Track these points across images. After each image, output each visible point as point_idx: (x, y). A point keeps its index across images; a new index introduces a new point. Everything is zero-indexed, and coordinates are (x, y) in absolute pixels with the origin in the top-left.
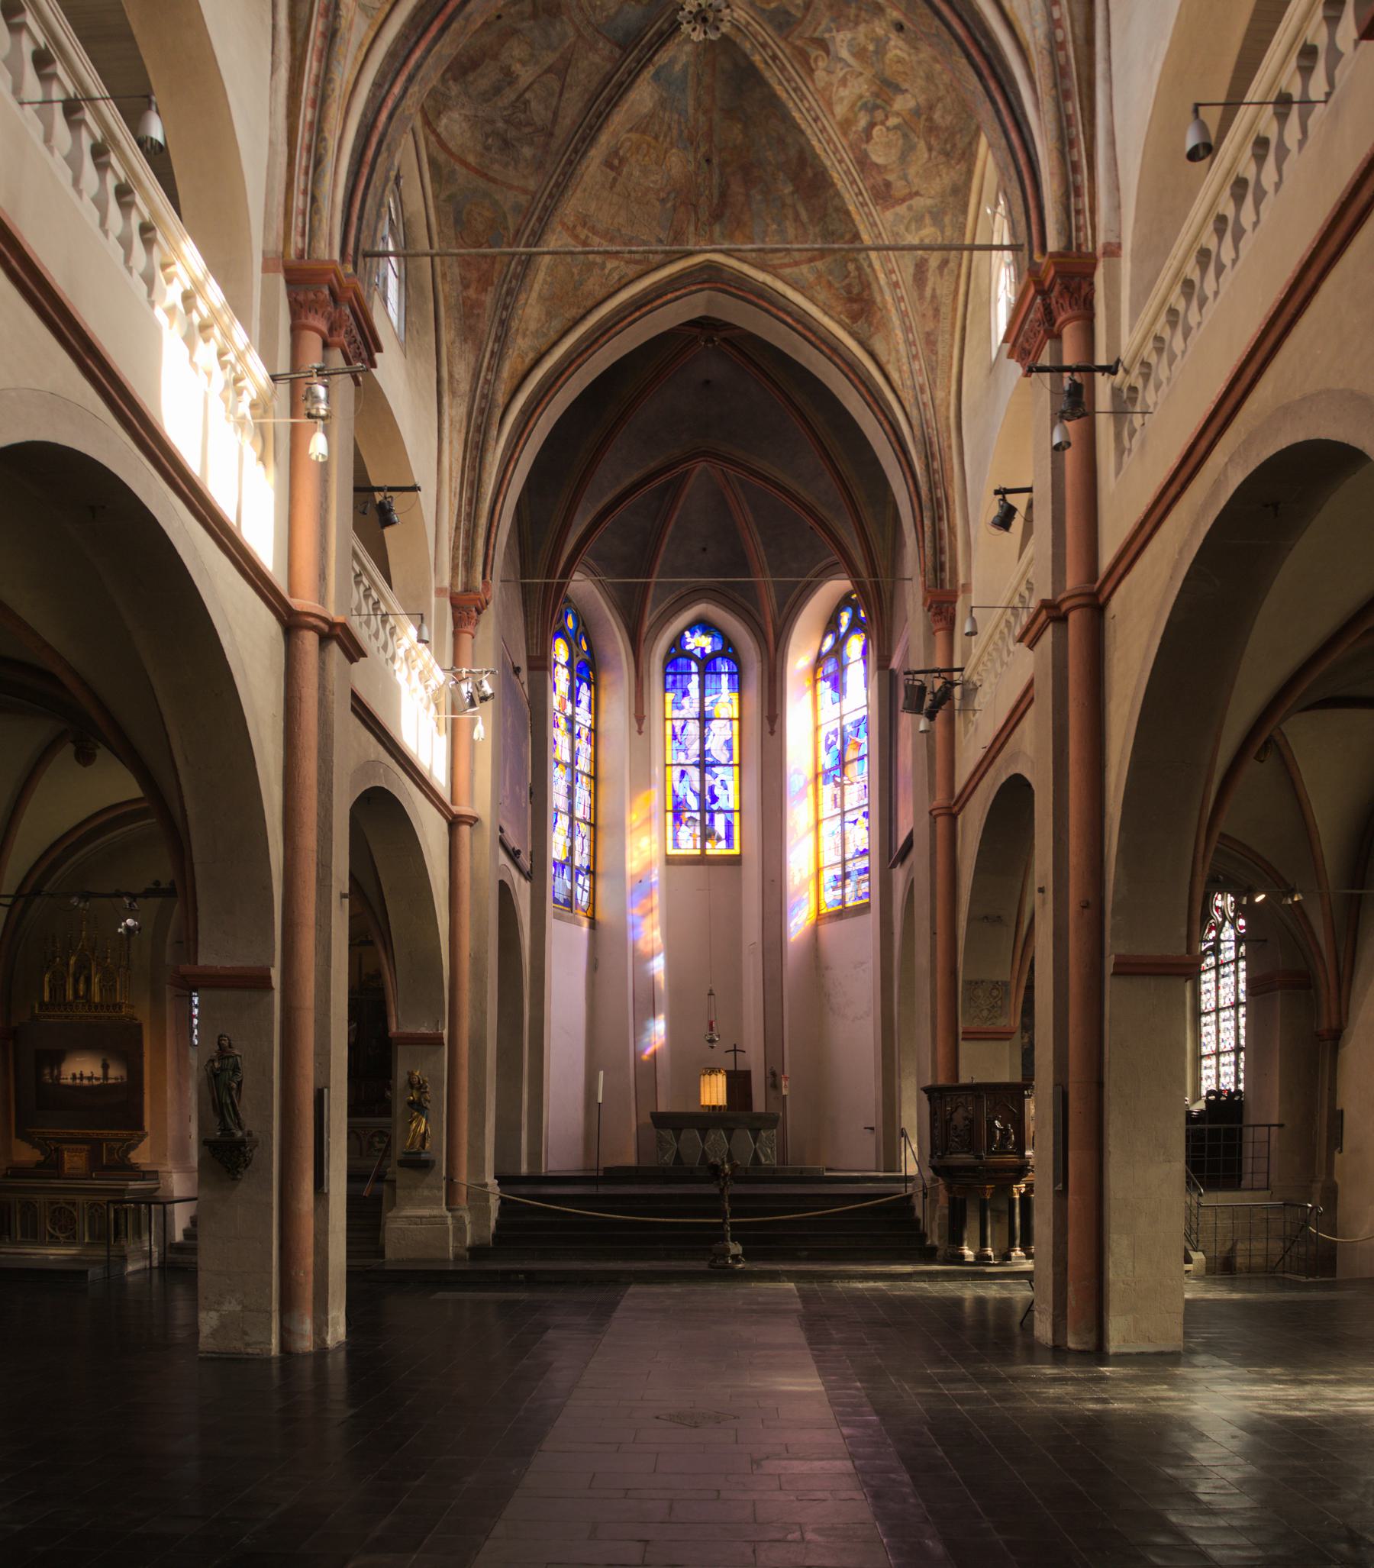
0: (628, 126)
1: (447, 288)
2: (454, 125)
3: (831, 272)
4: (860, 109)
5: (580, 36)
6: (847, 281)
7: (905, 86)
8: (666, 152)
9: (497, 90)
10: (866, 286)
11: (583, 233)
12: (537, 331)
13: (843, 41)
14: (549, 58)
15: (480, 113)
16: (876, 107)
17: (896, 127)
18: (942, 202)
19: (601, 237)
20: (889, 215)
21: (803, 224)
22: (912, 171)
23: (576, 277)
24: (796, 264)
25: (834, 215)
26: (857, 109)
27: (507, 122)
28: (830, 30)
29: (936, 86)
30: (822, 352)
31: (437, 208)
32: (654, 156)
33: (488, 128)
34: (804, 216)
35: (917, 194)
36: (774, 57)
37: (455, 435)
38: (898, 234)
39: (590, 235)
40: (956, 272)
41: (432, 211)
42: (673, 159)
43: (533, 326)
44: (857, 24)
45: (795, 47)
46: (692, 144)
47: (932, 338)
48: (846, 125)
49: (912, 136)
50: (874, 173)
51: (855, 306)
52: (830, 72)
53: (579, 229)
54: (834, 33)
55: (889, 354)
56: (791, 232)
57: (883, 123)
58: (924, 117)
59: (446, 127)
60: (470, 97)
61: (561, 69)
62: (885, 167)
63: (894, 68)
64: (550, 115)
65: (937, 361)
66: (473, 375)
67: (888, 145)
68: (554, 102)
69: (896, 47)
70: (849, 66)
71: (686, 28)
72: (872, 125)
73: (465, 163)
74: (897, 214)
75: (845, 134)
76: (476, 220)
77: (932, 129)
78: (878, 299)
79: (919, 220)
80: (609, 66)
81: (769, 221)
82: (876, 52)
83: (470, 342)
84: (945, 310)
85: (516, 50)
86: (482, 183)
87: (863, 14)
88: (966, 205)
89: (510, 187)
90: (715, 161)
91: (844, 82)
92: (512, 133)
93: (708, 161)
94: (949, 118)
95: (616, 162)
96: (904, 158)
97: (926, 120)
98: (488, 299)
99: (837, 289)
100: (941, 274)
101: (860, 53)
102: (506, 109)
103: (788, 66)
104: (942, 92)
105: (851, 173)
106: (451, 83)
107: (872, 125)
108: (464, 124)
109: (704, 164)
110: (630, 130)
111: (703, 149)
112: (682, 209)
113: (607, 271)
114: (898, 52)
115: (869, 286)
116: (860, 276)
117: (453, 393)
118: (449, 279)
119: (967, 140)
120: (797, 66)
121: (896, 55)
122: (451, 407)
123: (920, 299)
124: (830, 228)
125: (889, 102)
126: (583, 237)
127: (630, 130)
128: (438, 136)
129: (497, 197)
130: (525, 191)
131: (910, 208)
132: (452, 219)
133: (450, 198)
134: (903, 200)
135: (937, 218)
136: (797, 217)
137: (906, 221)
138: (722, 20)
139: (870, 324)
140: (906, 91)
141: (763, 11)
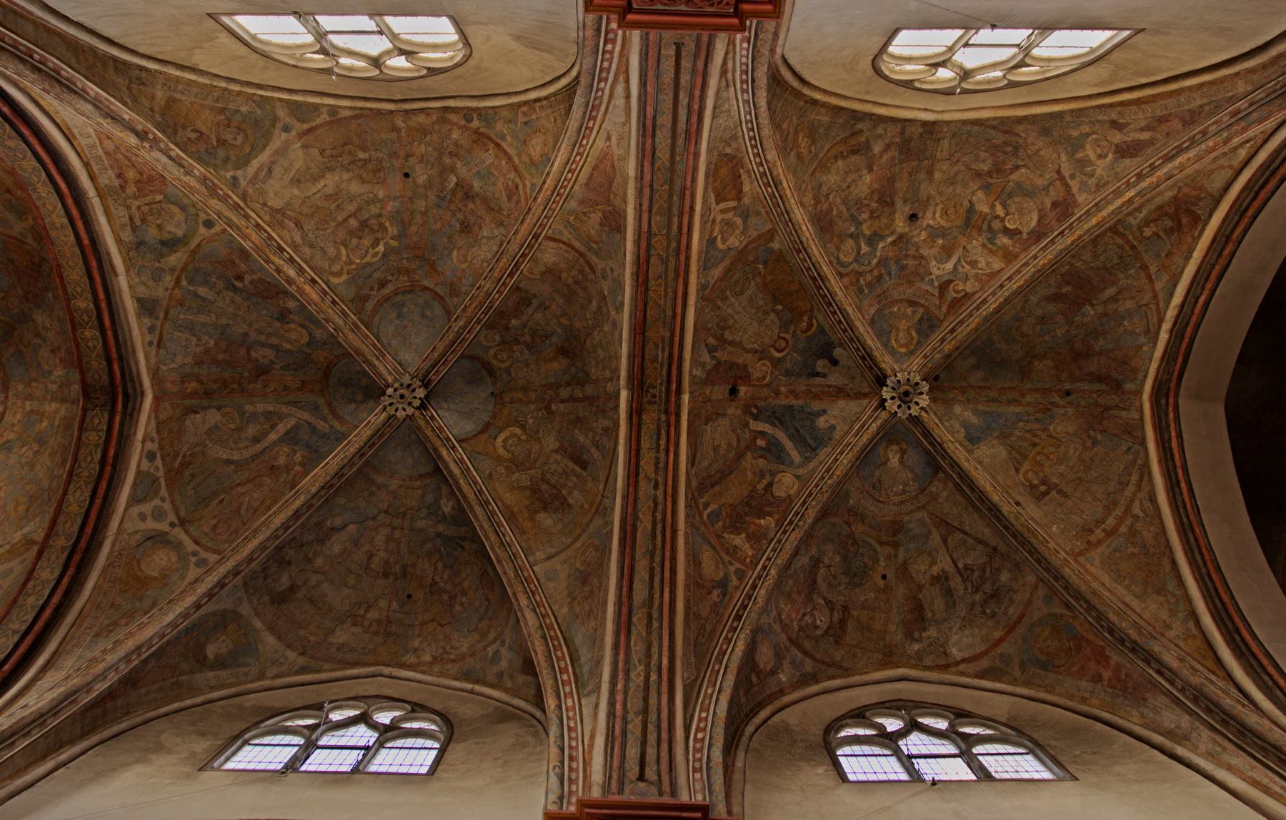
0: (1013, 472)
1: (1095, 701)
2: (961, 643)
3: (1158, 256)
4: (995, 244)
5: (924, 507)
6: (1162, 234)
7: (966, 203)
8: (1051, 436)
9: (949, 593)
10: (1161, 212)
11: (1099, 533)
12: (1170, 610)
13: (939, 269)
14: (936, 538)
15: (962, 614)
16: (990, 228)
17: (1004, 206)
18: (1061, 144)
19: (1110, 514)
20: (1081, 198)
21: (1119, 292)
22: (1040, 182)
23: (1136, 550)
24: (1155, 296)
25: (1102, 258)
26: (994, 248)
27: (977, 591)
28: (932, 281)
29: (957, 173)
30: (1233, 254)
31: (1026, 684)
32: (1052, 449)
33: (978, 609)
34: (1111, 291)
35: (1059, 172)
36: (952, 331)
37: (1225, 757)
38: (1097, 185)
39: (1103, 526)
40: (1119, 108)
41: (1019, 690)
42: (1058, 429)
43: (1164, 614)
44: (922, 257)
45: (948, 312)
46: (1049, 410)
47: (1187, 118)
48: (1009, 257)
49: (1009, 188)
50: (1046, 222)
51: (1184, 221)
52: (967, 279)
53: (1093, 538)
54: (933, 277)
55: (1223, 167)
56: (1129, 304)
57: (1003, 220)
58: (989, 180)
59: (960, 650)
60: (945, 620)
61: (947, 528)
62: (1040, 211)
63: (953, 217)
64: (980, 547)
65: (1209, 104)
66: (1177, 704)
67: (1021, 211)
68: (970, 541)
69: (934, 218)
70: (959, 260)
71: (914, 411)
72: (1006, 231)
73: (1000, 641)
74: (1080, 189)
75: (1016, 257)
76: (1048, 646)
77: (997, 170)
78: (1169, 194)
79: (1083, 163)
80: (950, 484)
81: (1122, 329)
82: (943, 236)
83: (1148, 695)
84: (1157, 110)
85: (921, 570)
86: (1021, 629)
87: (911, 253)
88: (1051, 116)
89: (1030, 602)
90: (1068, 386)
91: (973, 264)
92: (988, 588)
93: (1068, 393)
94: (983, 155)
95: (1043, 488)
96: (1029, 194)
97: (991, 177)
98: (1115, 658)
99: (1172, 245)
100: (1127, 125)
101: (947, 252)
102: (966, 589)
103: (961, 317)
104: (961, 167)
105: (1046, 246)
106: (924, 634)
107: (1006, 231)
108: (966, 632)
109: (1069, 399)
110: (1017, 471)
111: (1056, 399)
112: (1105, 422)
113: (1141, 514)
114: (938, 215)
115: (1160, 207)
116: (1155, 220)
117: (1183, 739)
118: (1088, 695)
119: (993, 133)
120: (964, 308)
121: (941, 216)
122: (1194, 749)
123: (1153, 144)
124: (1116, 261)
125: (984, 217)
126: (1103, 534)
127: (1017, 471)
128: (964, 660)
129: (1035, 619)
130: (1036, 587)
131: (1073, 177)
132: (1042, 672)
133: (1022, 667)
134: (1067, 185)
135: (1075, 146)
136: (1114, 299)
137: (1085, 179)
138: (908, 380)
139: (1199, 199)
140: (970, 202)
141: (918, 342)
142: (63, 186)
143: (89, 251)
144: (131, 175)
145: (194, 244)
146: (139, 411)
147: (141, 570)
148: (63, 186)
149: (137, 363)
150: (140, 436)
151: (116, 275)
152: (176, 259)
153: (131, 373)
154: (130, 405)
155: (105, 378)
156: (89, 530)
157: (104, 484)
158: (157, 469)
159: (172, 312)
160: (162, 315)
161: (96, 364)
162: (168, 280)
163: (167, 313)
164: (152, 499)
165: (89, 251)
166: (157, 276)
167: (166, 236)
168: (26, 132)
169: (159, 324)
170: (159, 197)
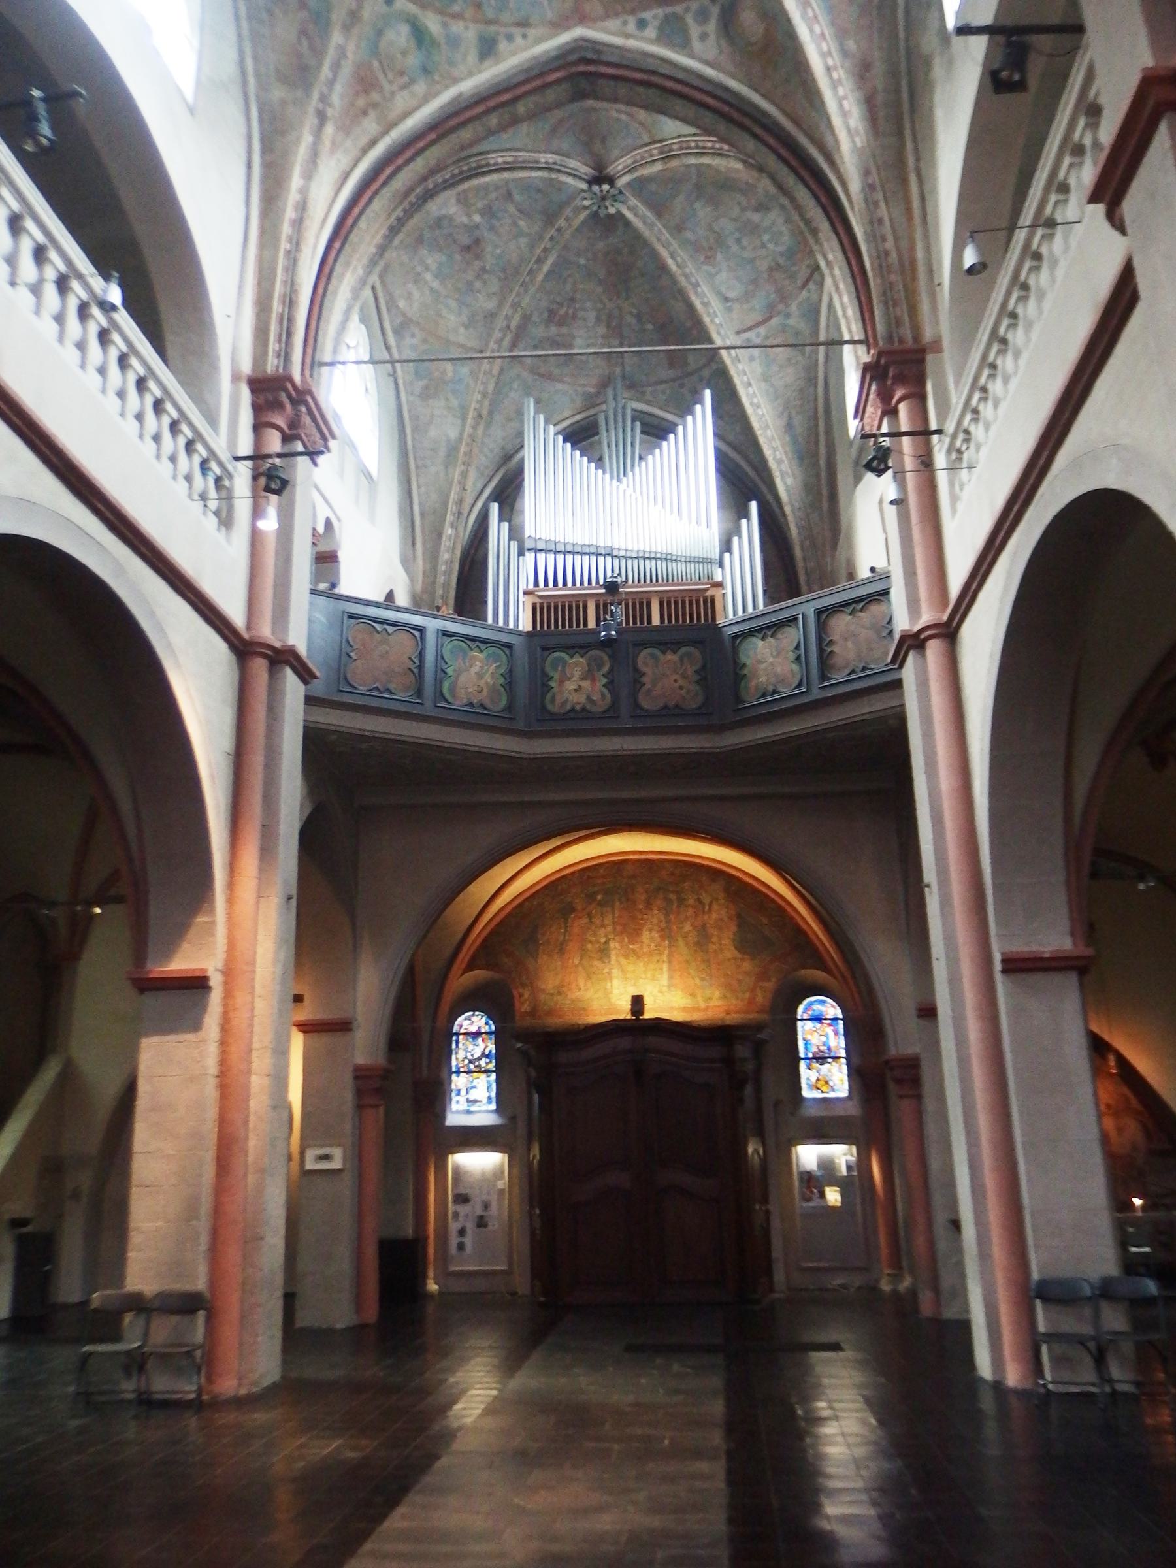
142: (388, 171)
143: (440, 131)
144: (361, 102)
145: (413, 9)
146: (594, 42)
147: (755, 44)
148: (388, 171)
149: (547, 52)
150: (618, 41)
151: (460, 95)
152: (433, 23)
153: (556, 58)
154: (590, 55)
155: (564, 86)
156: (711, 101)
157: (669, 84)
158: (655, 17)
159: (490, 14)
160: (493, 28)
161: (551, 95)
162: (457, 27)
163: (489, 22)
164: (686, 24)
165: (440, 131)
166: (454, 42)
167: (413, 44)
168: (350, 221)
169: (502, 30)
170: (376, 64)
